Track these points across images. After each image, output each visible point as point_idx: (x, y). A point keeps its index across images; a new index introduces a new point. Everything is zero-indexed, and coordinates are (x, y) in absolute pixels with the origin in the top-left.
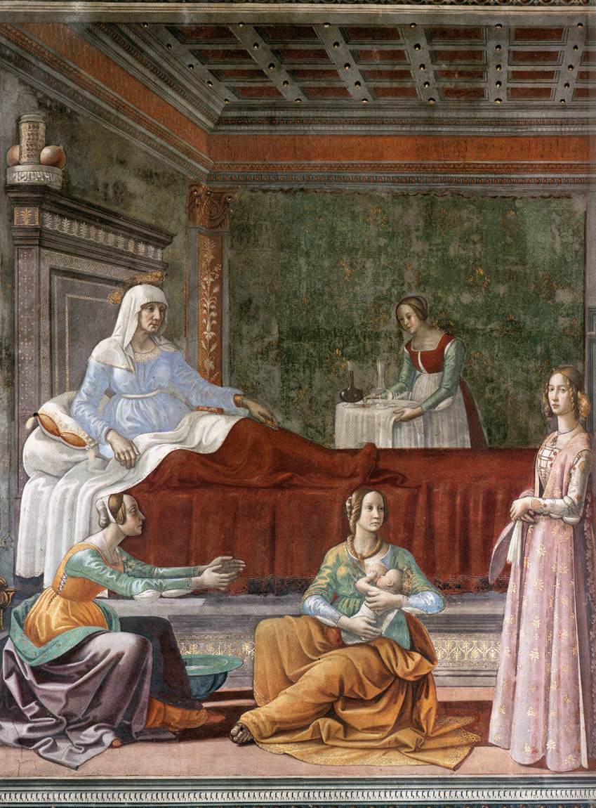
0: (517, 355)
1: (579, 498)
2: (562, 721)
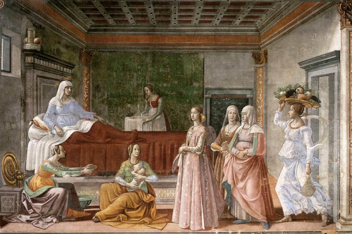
1: (201, 146)
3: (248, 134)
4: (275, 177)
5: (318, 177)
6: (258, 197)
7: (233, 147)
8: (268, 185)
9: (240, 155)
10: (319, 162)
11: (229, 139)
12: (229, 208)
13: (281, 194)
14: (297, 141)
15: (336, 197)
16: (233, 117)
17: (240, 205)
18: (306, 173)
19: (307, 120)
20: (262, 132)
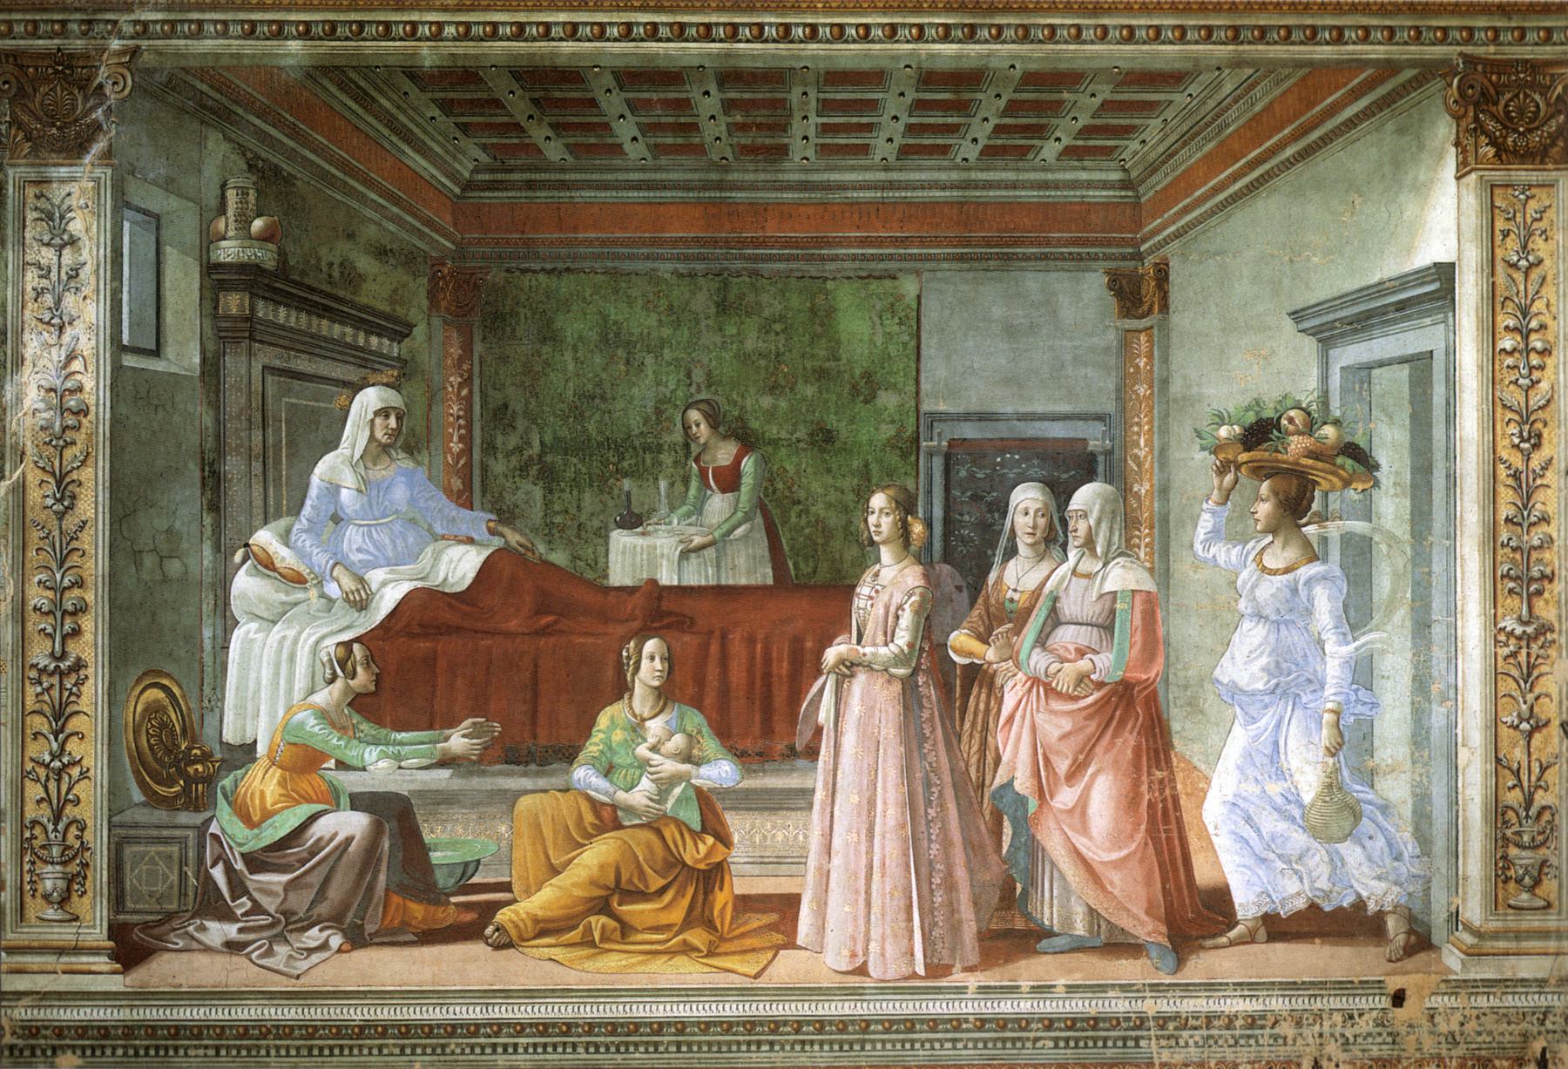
0: (829, 471)
1: (911, 645)
2: (888, 918)
3: (1094, 597)
4: (1198, 764)
5: (1370, 764)
6: (1133, 846)
7: (1033, 648)
8: (1176, 799)
9: (1065, 680)
10: (1374, 705)
11: (1021, 618)
12: (1018, 891)
13: (1224, 831)
14: (1286, 623)
15: (1440, 845)
16: (1035, 527)
17: (1063, 877)
18: (1322, 752)
19: (1324, 540)
20: (1149, 585)
